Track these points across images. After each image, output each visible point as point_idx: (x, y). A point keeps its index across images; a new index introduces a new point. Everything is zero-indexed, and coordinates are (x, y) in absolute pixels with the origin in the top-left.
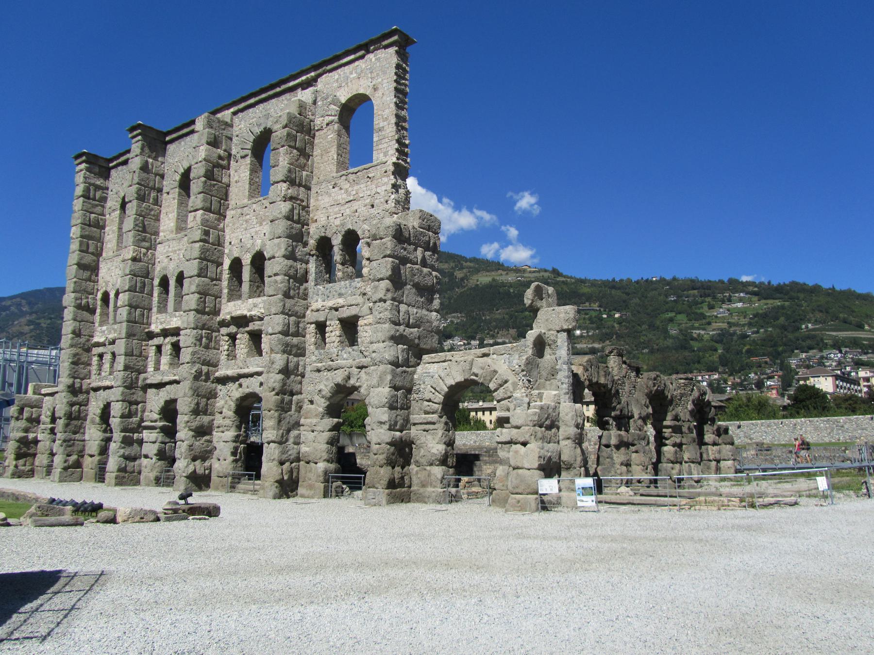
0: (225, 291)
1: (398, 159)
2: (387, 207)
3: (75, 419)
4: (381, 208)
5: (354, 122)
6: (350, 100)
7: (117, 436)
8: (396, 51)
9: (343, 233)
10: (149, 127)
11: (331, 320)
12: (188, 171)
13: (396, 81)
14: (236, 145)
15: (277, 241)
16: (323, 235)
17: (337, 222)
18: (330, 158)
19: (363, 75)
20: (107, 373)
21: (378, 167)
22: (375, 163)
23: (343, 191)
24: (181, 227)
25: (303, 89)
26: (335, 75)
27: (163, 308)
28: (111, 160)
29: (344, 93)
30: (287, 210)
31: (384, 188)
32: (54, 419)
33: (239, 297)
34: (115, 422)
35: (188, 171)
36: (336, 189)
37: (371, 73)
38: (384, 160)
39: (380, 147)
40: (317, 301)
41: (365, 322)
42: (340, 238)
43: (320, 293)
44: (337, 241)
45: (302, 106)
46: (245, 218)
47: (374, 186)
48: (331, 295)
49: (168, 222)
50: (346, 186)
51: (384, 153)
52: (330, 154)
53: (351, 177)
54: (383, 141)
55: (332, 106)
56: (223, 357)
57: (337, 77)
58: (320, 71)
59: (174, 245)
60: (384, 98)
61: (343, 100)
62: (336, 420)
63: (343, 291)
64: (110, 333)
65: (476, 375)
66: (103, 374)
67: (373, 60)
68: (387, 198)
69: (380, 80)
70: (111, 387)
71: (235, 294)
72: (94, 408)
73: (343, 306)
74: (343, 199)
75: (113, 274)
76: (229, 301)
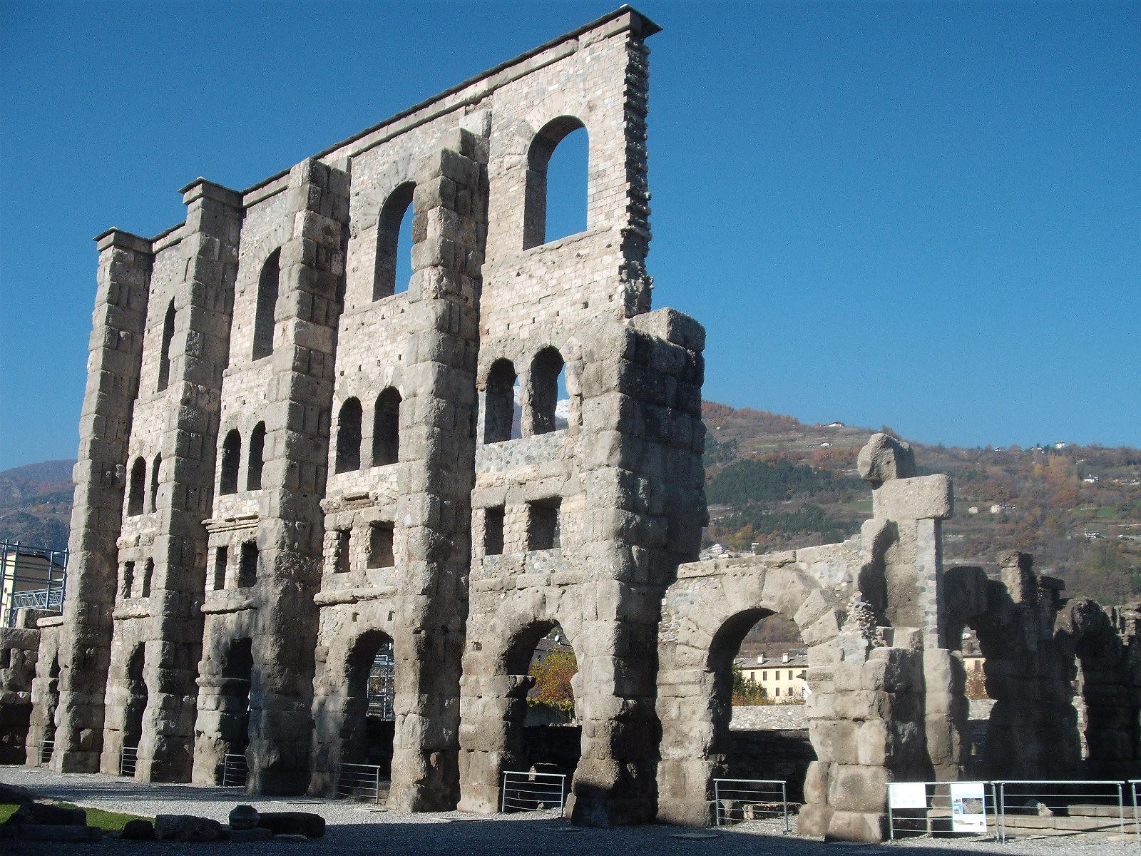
0: (333, 454)
1: (630, 223)
2: (613, 305)
3: (90, 667)
4: (601, 308)
7: (155, 699)
8: (628, 45)
9: (535, 352)
11: (514, 502)
12: (276, 255)
13: (625, 94)
14: (355, 208)
15: (421, 366)
16: (500, 356)
17: (525, 334)
18: (513, 226)
19: (569, 85)
20: (141, 593)
22: (590, 230)
23: (534, 281)
24: (263, 346)
25: (466, 113)
26: (522, 87)
27: (229, 486)
28: (155, 241)
29: (538, 117)
30: (440, 312)
31: (606, 273)
32: (55, 670)
33: (355, 465)
34: (151, 675)
35: (276, 255)
36: (523, 277)
37: (584, 80)
38: (606, 224)
39: (600, 203)
40: (488, 470)
41: (573, 505)
42: (529, 359)
43: (494, 456)
44: (523, 368)
45: (467, 140)
47: (588, 271)
48: (513, 462)
49: (240, 340)
50: (540, 271)
52: (513, 218)
53: (549, 257)
54: (605, 194)
55: (517, 138)
56: (328, 567)
57: (525, 90)
58: (497, 79)
59: (251, 378)
60: (607, 122)
61: (537, 130)
62: (520, 677)
64: (145, 525)
65: (771, 599)
66: (133, 594)
68: (611, 291)
69: (599, 93)
70: (147, 615)
71: (349, 460)
72: (120, 651)
73: (535, 479)
74: (534, 293)
75: (154, 428)
76: (338, 471)
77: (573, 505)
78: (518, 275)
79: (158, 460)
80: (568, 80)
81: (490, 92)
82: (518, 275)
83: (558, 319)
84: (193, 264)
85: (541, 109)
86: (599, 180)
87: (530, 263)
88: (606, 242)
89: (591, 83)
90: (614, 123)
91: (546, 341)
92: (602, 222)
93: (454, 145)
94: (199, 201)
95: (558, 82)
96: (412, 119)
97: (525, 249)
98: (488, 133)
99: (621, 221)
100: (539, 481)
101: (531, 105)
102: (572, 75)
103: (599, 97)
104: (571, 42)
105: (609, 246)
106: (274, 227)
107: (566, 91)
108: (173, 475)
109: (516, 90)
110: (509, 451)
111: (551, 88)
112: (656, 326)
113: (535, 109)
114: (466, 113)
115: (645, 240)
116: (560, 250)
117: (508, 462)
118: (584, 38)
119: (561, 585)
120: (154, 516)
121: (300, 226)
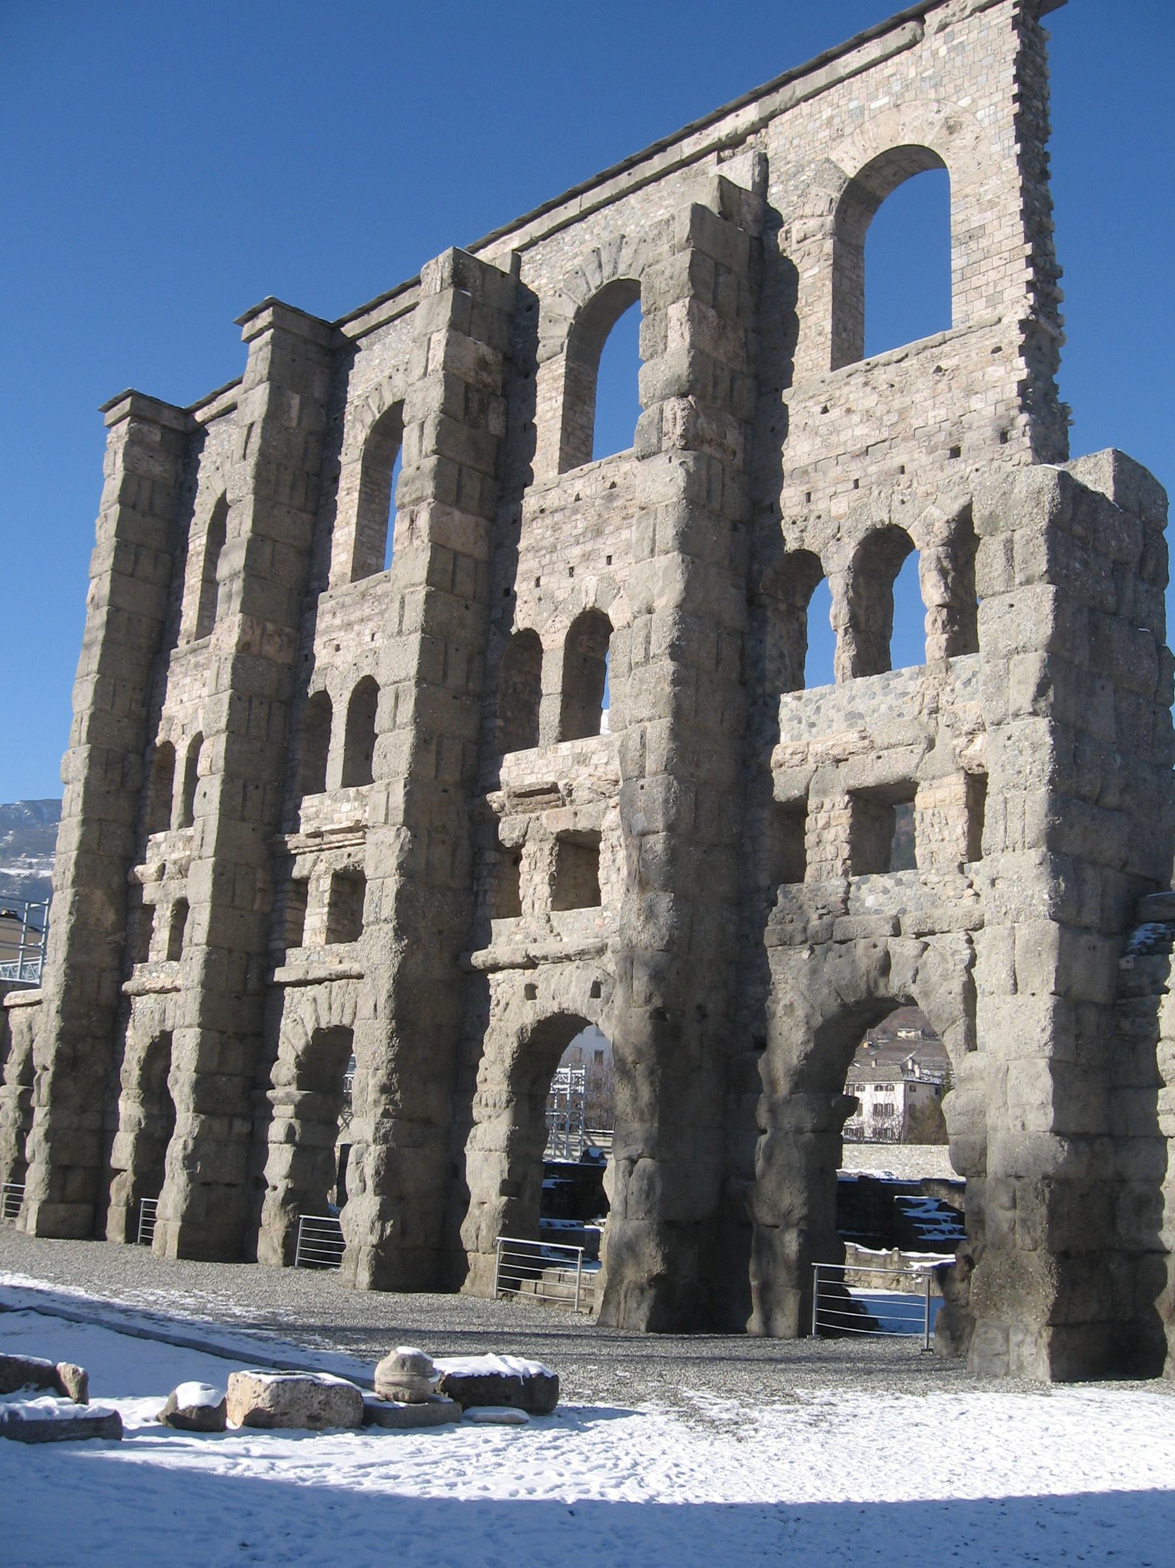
5: (878, 231)
6: (870, 169)
9: (860, 535)
10: (295, 310)
13: (1016, 98)
15: (661, 561)
21: (972, 339)
22: (958, 325)
23: (855, 418)
26: (822, 108)
29: (853, 152)
37: (936, 86)
38: (988, 315)
39: (976, 281)
41: (940, 794)
46: (549, 521)
48: (822, 723)
51: (989, 299)
57: (827, 113)
60: (983, 147)
61: (851, 170)
63: (860, 706)
67: (943, 51)
77: (940, 794)
78: (825, 410)
79: (198, 740)
80: (907, 87)
81: (764, 122)
82: (825, 410)
83: (904, 479)
84: (257, 430)
85: (858, 139)
86: (973, 245)
87: (846, 390)
88: (990, 344)
89: (950, 88)
90: (996, 148)
91: (880, 516)
92: (981, 312)
93: (708, 198)
94: (268, 335)
95: (888, 93)
96: (624, 181)
97: (833, 369)
98: (762, 184)
99: (1017, 304)
100: (873, 755)
101: (840, 135)
102: (913, 80)
103: (966, 110)
104: (911, 25)
105: (998, 349)
106: (387, 374)
107: (903, 107)
108: (221, 763)
109: (811, 115)
110: (813, 706)
111: (874, 105)
112: (1096, 473)
113: (848, 140)
114: (720, 160)
115: (1055, 341)
116: (903, 364)
117: (813, 725)
118: (933, 18)
119: (919, 935)
120: (190, 831)
121: (438, 354)
